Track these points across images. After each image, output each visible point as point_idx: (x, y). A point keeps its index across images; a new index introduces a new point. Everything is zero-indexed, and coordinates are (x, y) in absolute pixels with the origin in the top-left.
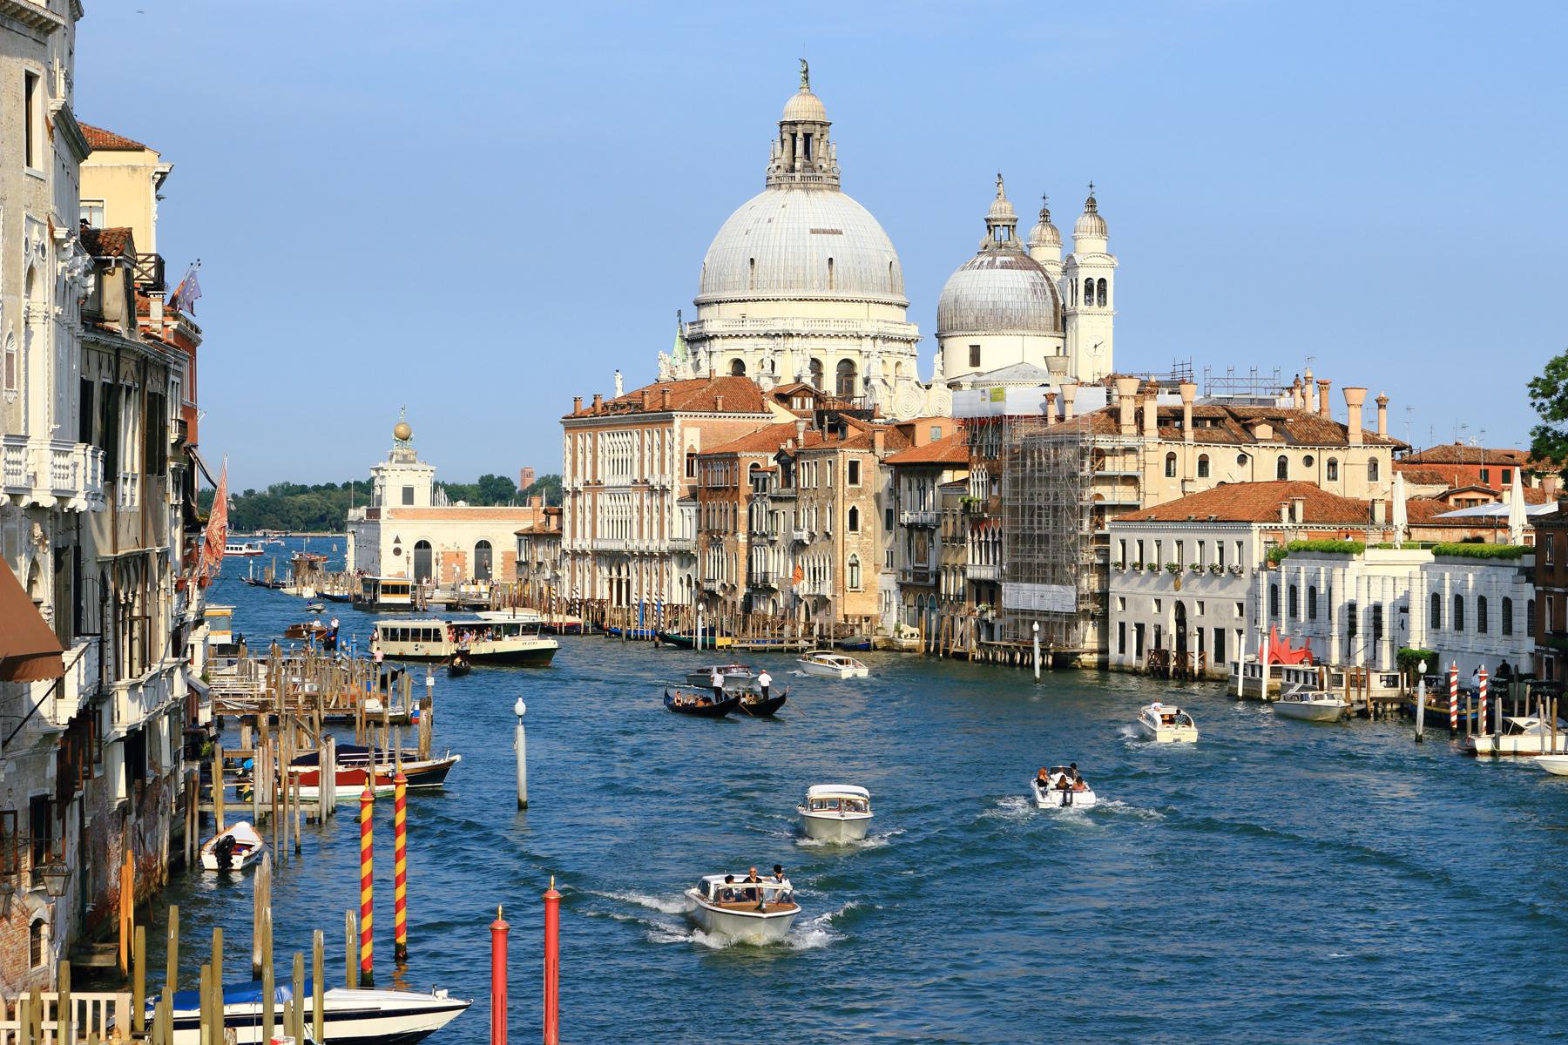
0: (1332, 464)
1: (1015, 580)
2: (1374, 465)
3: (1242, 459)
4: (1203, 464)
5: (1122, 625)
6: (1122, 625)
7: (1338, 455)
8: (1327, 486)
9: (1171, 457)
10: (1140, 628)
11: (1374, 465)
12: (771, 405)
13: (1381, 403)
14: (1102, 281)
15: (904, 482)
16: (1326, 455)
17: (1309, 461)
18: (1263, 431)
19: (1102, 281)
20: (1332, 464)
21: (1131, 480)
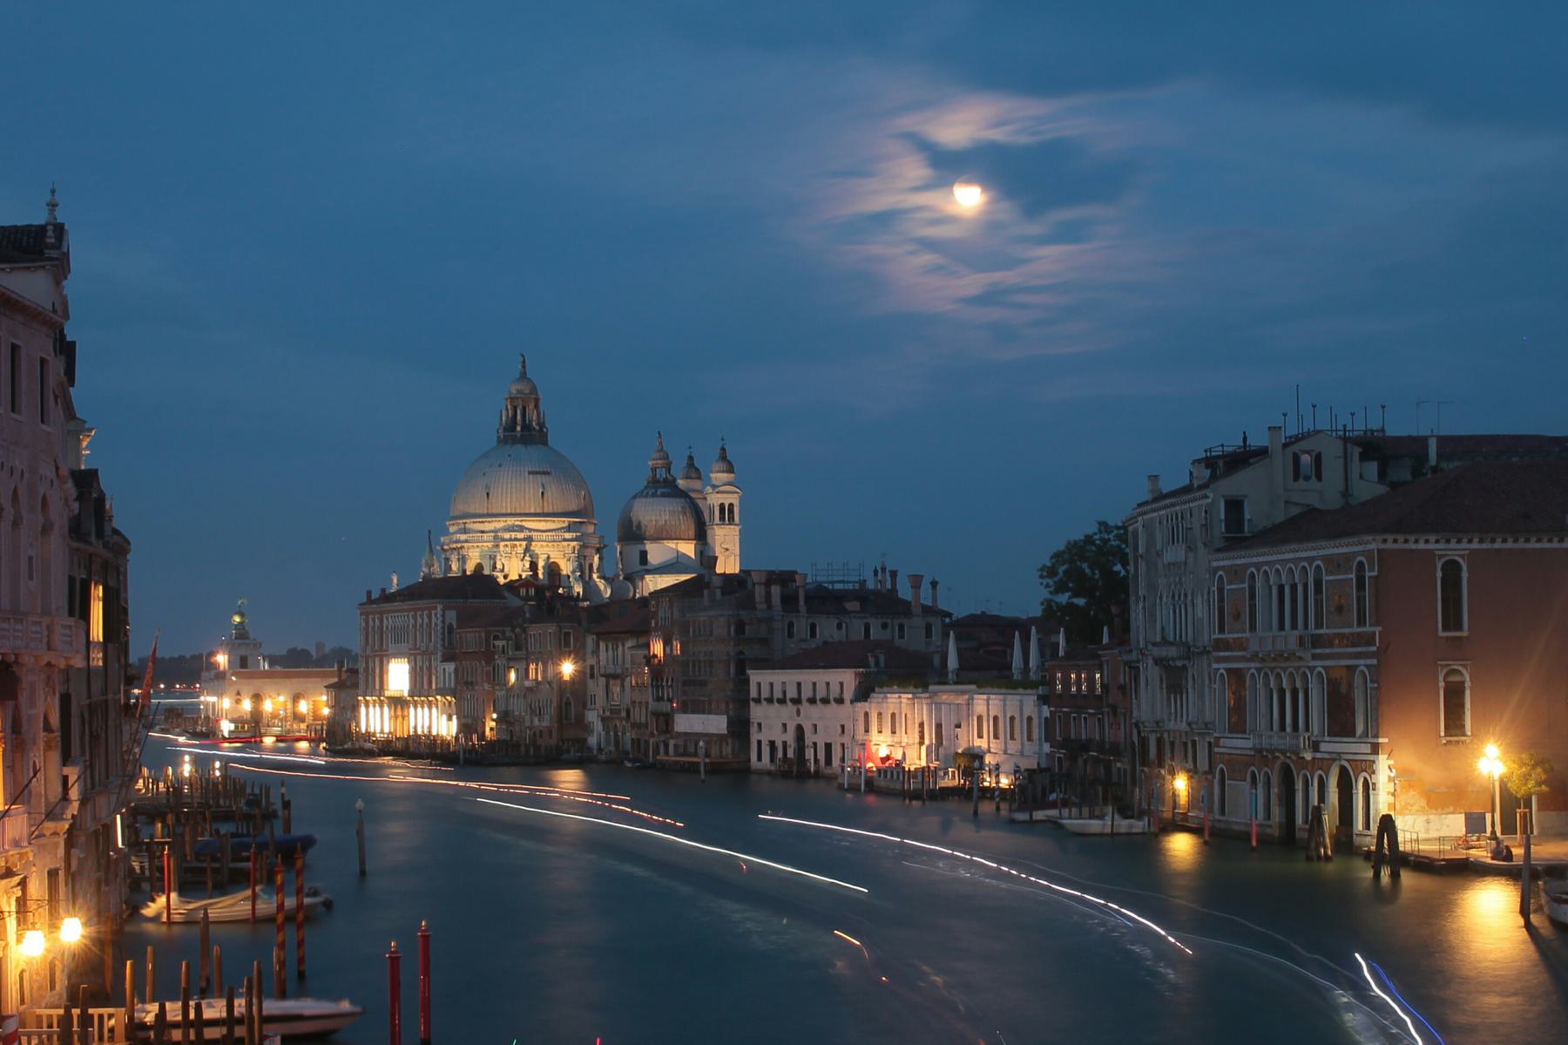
0: (901, 627)
1: (685, 712)
2: (929, 628)
3: (839, 627)
4: (813, 627)
5: (759, 742)
6: (759, 742)
7: (905, 621)
8: (898, 642)
9: (791, 625)
10: (772, 743)
11: (929, 628)
12: (506, 594)
13: (934, 584)
14: (731, 505)
15: (602, 645)
16: (897, 622)
17: (884, 626)
18: (853, 606)
19: (731, 505)
20: (901, 627)
21: (764, 642)
